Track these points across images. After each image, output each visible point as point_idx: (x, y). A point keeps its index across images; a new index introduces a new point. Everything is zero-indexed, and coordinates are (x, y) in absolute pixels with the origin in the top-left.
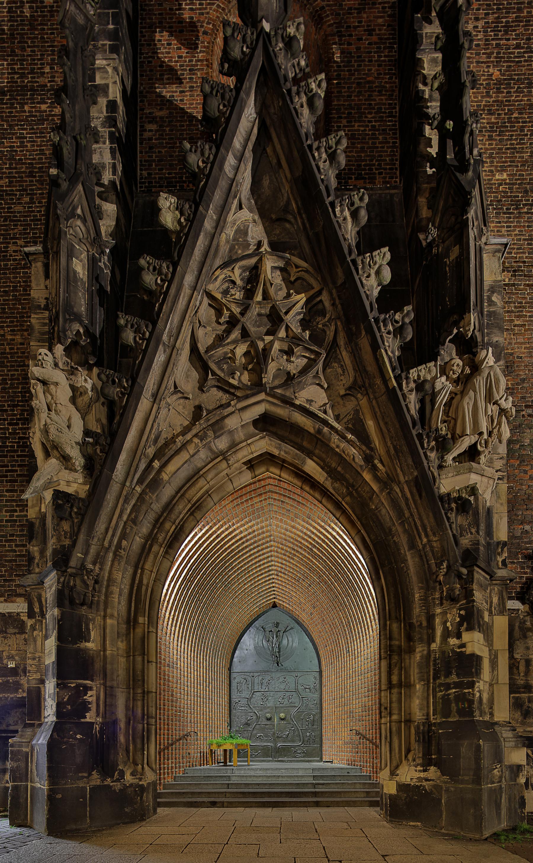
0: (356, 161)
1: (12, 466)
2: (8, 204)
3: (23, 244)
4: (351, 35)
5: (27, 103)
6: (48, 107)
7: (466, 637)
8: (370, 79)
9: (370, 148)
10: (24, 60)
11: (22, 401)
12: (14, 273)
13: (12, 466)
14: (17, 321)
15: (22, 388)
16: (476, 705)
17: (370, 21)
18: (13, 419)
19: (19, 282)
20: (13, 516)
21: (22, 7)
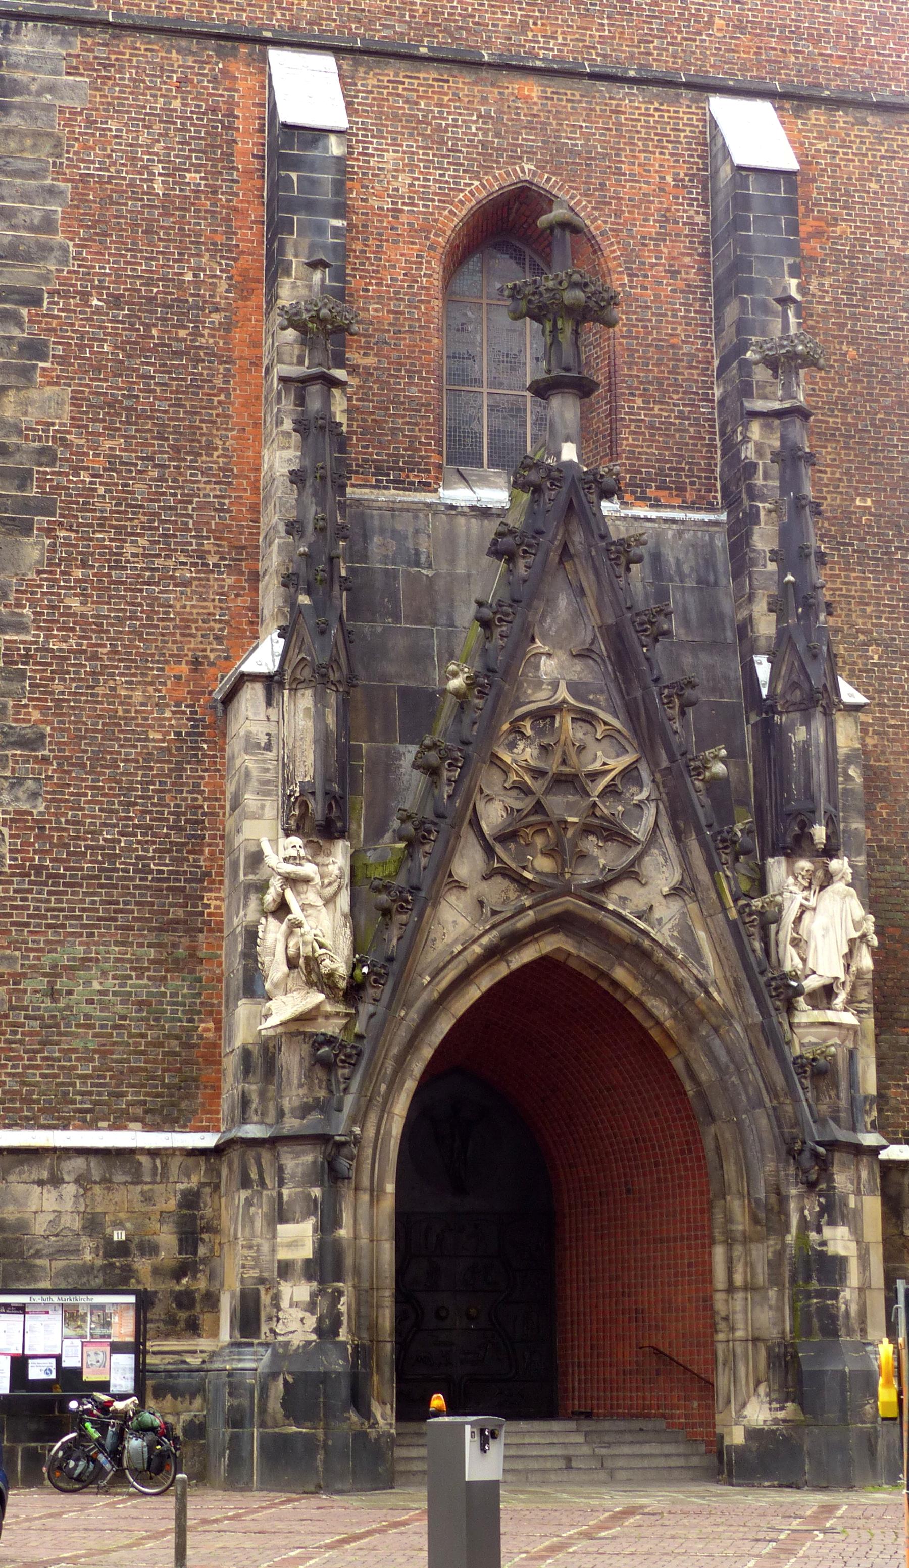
0: (658, 461)
1: (126, 903)
2: (124, 478)
3: (147, 544)
4: (646, 276)
5: (155, 325)
6: (190, 334)
7: (827, 1232)
8: (674, 341)
9: (677, 443)
10: (152, 259)
11: (141, 797)
12: (132, 590)
13: (126, 903)
14: (137, 668)
15: (143, 776)
16: (841, 1321)
17: (673, 259)
18: (127, 826)
19: (140, 605)
20: (125, 986)
21: (151, 181)
